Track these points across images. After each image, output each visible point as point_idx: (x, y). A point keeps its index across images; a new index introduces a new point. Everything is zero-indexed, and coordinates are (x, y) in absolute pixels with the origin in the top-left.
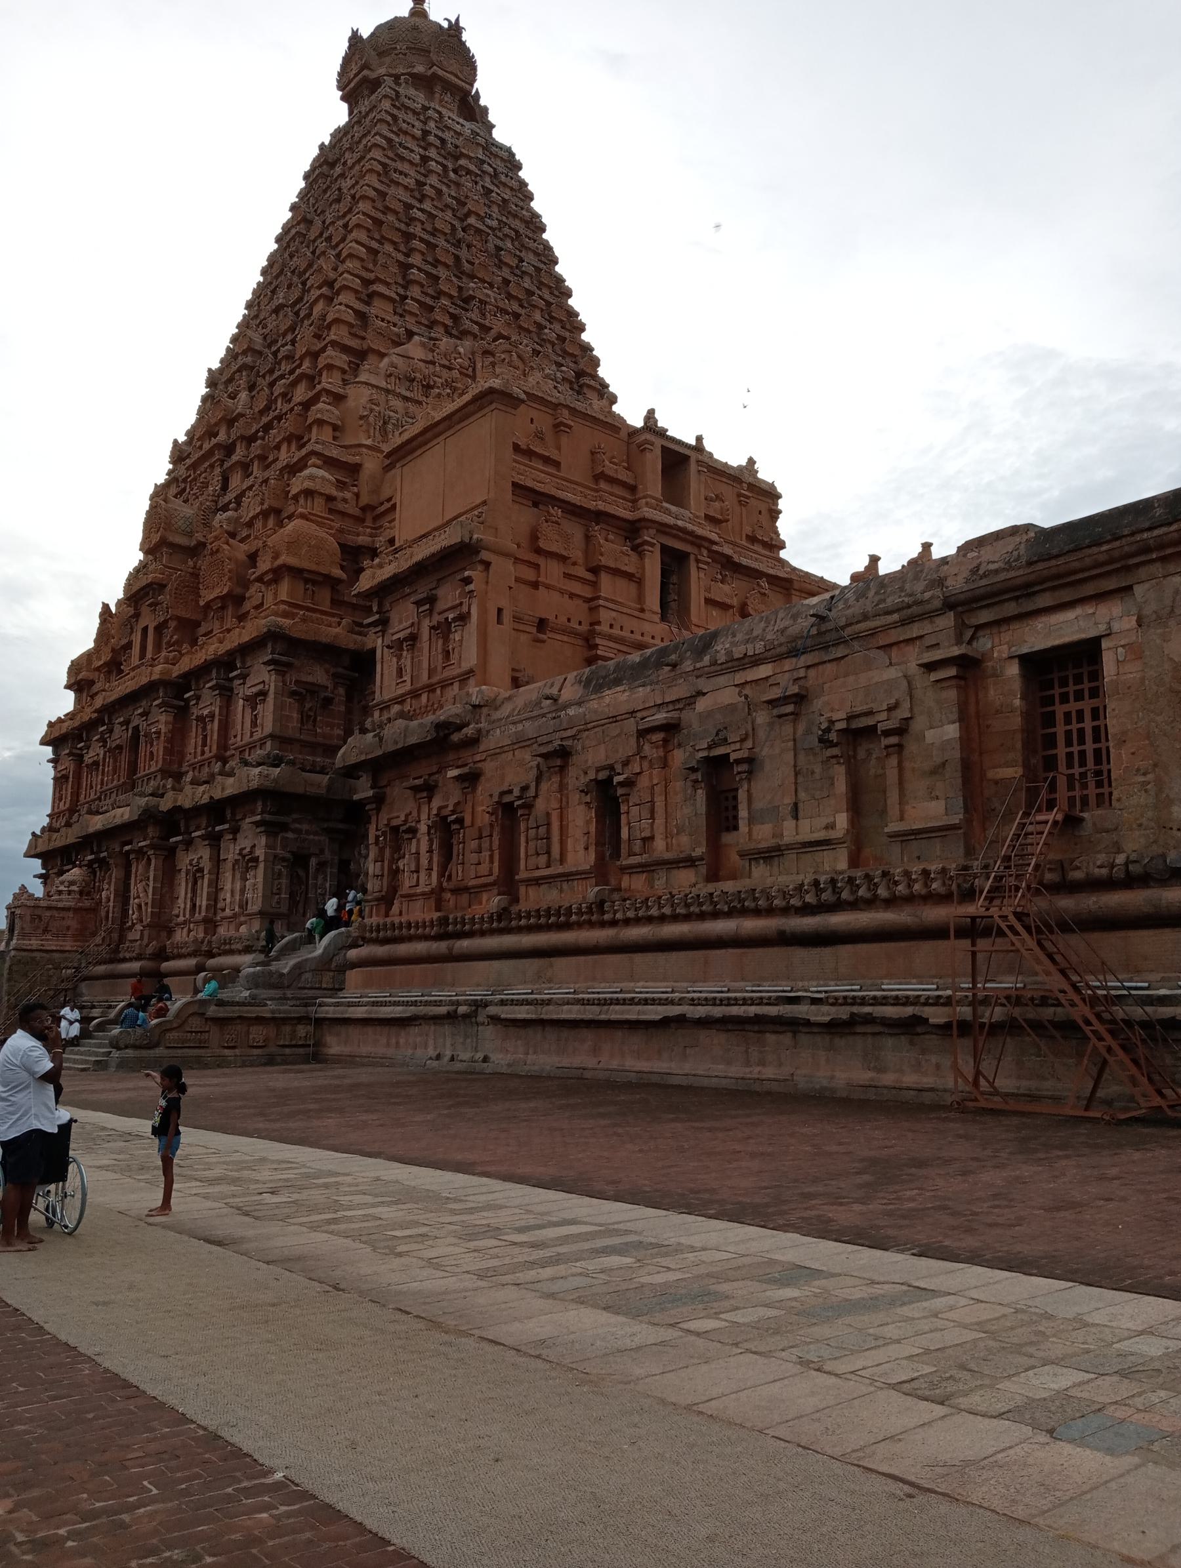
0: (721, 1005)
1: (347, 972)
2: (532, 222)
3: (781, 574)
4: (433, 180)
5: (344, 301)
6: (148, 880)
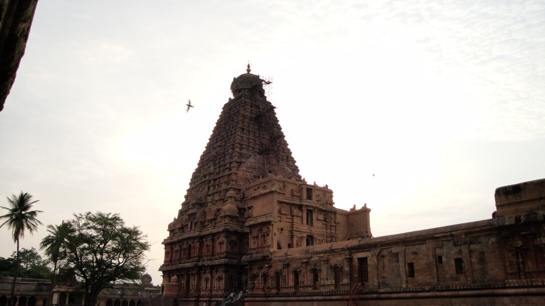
6: (195, 280)
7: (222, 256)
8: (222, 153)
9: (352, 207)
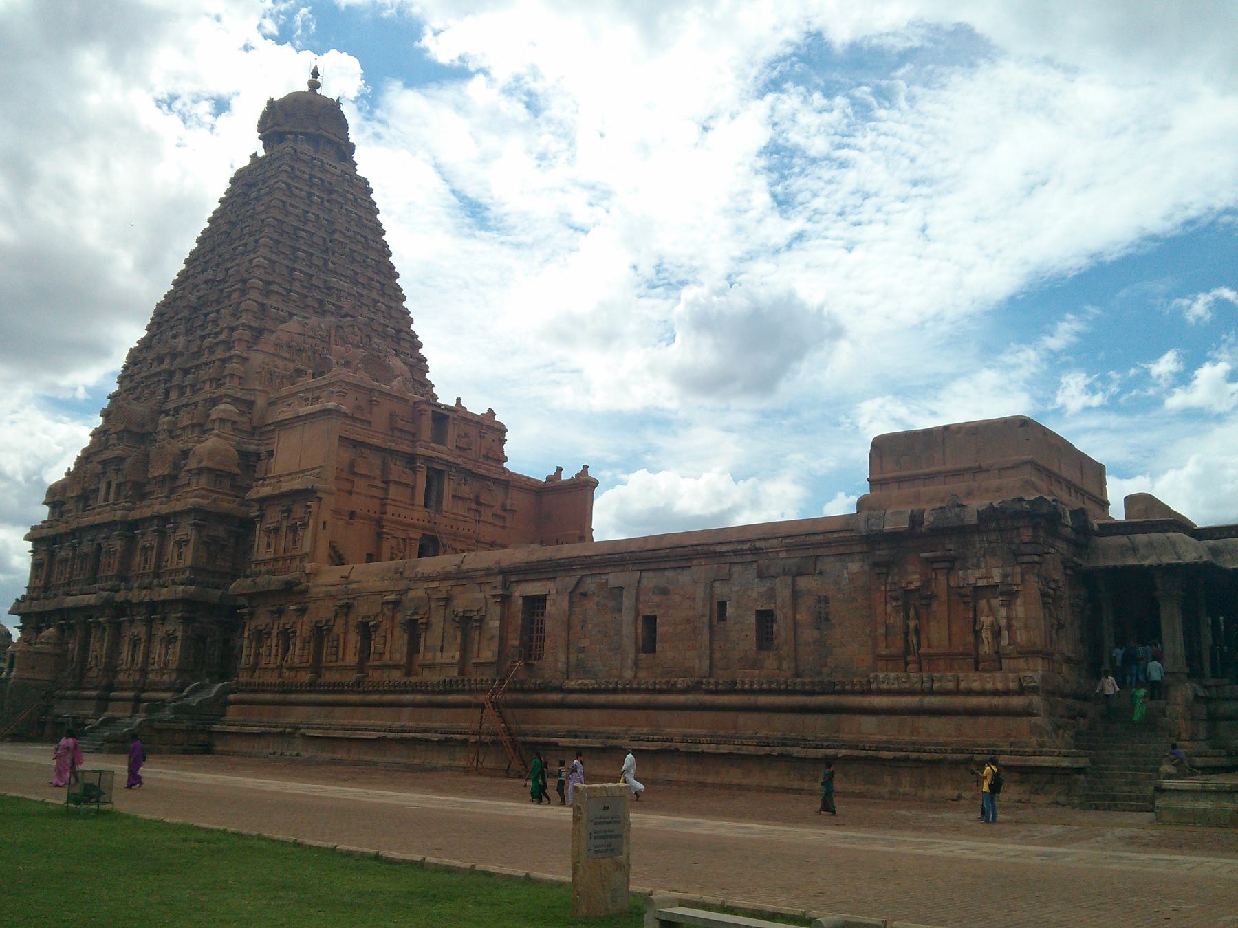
2: (377, 229)
5: (252, 297)
6: (103, 641)
7: (181, 577)
8: (213, 301)
9: (552, 472)
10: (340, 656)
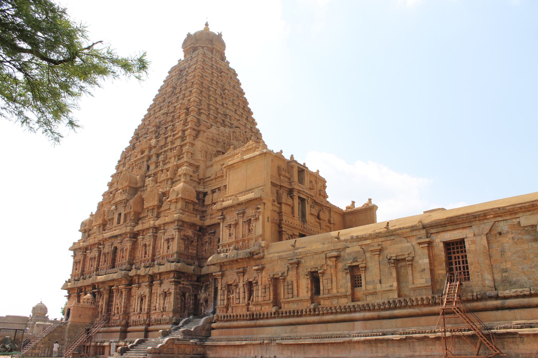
0: (363, 337)
1: (212, 331)
3: (328, 206)
4: (215, 79)
8: (169, 121)
9: (349, 204)
10: (295, 292)
